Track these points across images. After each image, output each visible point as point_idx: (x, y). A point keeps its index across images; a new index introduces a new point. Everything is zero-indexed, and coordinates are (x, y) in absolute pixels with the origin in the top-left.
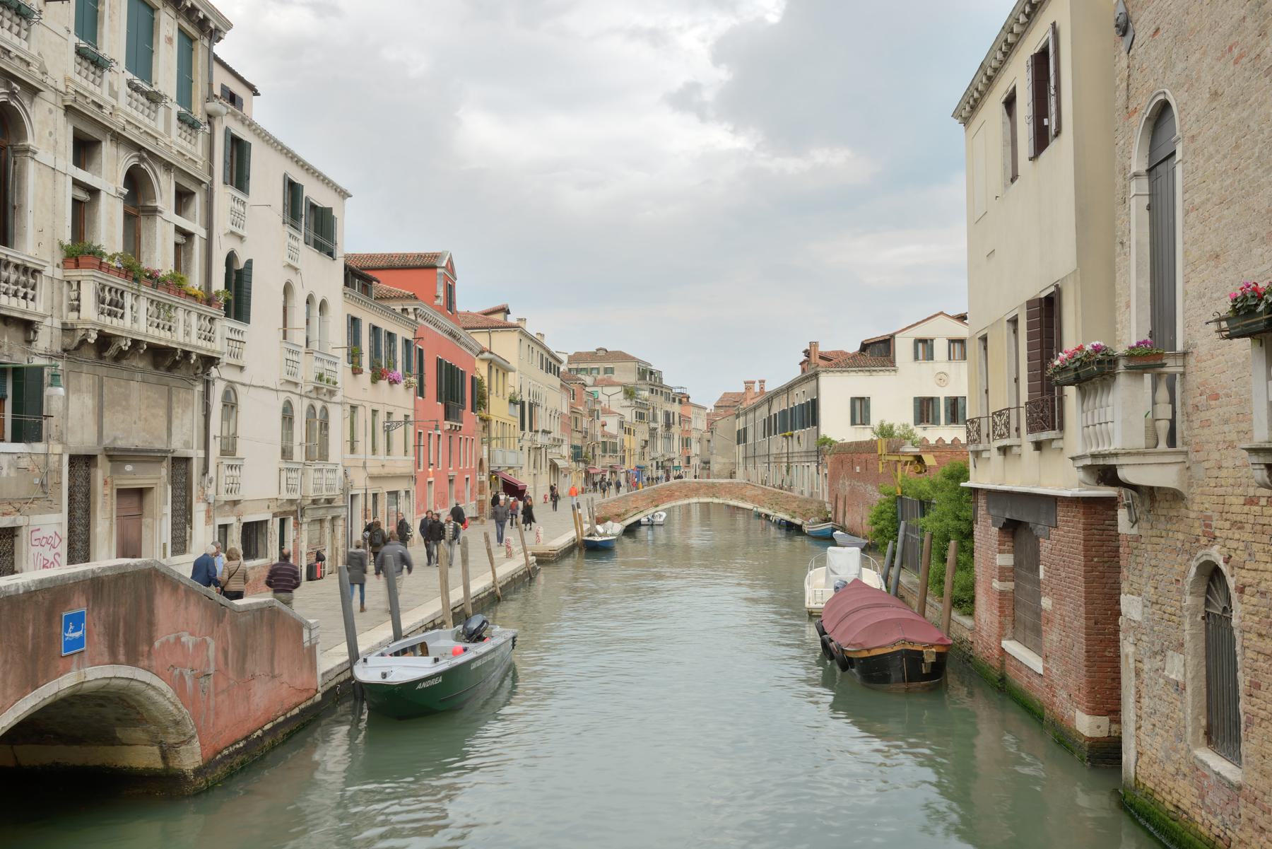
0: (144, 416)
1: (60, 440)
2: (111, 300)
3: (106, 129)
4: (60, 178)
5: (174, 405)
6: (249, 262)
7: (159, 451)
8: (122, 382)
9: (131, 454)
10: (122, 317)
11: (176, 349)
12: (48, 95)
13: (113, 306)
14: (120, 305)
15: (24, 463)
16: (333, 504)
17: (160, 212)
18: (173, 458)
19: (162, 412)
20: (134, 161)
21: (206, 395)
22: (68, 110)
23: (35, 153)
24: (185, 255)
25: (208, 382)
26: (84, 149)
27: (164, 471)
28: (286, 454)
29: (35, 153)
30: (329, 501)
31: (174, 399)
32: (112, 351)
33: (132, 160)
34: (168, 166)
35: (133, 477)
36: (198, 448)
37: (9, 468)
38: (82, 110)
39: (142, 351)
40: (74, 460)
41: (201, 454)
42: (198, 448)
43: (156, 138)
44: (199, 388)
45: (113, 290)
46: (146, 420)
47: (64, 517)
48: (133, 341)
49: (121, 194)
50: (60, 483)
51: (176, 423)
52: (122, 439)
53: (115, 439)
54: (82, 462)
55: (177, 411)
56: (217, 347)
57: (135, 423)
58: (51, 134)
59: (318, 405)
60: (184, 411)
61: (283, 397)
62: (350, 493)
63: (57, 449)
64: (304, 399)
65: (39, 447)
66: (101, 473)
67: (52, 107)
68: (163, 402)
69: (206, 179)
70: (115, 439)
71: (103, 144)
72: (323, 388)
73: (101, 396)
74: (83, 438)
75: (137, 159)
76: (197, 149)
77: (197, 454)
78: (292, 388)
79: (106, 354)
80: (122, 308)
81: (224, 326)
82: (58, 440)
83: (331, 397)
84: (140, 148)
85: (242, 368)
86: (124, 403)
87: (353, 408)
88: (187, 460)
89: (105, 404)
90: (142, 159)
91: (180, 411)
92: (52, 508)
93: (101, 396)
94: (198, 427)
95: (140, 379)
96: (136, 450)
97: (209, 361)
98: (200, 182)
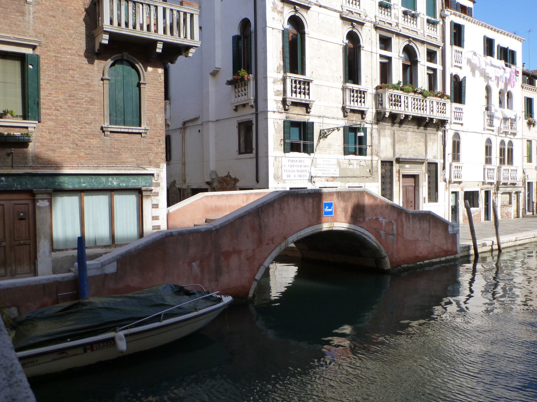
0: (413, 146)
1: (377, 155)
2: (395, 100)
3: (393, 32)
4: (374, 55)
5: (428, 141)
6: (465, 78)
7: (420, 159)
8: (404, 132)
9: (407, 160)
10: (400, 106)
11: (426, 117)
12: (367, 24)
13: (397, 101)
14: (399, 101)
15: (363, 163)
16: (516, 186)
17: (419, 62)
18: (429, 163)
19: (422, 144)
20: (407, 43)
21: (444, 137)
22: (376, 28)
23: (363, 47)
24: (433, 78)
25: (445, 131)
26: (385, 43)
27: (424, 167)
28: (488, 161)
29: (363, 47)
30: (514, 184)
31: (428, 138)
32: (398, 120)
33: (406, 43)
34: (423, 42)
35: (409, 169)
36: (441, 159)
37: (357, 165)
38: (382, 27)
39: (410, 119)
40: (383, 162)
41: (442, 161)
42: (441, 159)
43: (417, 32)
44: (440, 133)
45: (396, 96)
46: (415, 147)
47: (379, 184)
48: (405, 115)
49: (401, 57)
50: (378, 171)
51: (429, 149)
52: (404, 155)
53: (401, 155)
54: (387, 164)
55: (430, 144)
56: (447, 115)
57: (410, 148)
58: (370, 39)
59: (507, 141)
60: (433, 143)
61: (485, 137)
62: (527, 181)
63: (375, 158)
64: (498, 137)
65: (368, 158)
66: (396, 167)
67: (370, 28)
68: (423, 140)
69: (442, 45)
70: (401, 155)
71: (392, 39)
72: (508, 132)
73: (394, 138)
74: (388, 155)
75: (408, 42)
76: (438, 34)
77: (440, 162)
78: (491, 132)
79: (396, 121)
80: (400, 102)
81: (451, 107)
82: (376, 155)
83: (514, 137)
84: (408, 37)
85: (462, 124)
86: (405, 140)
87: (530, 141)
88: (436, 164)
89: (396, 141)
90: (410, 41)
91: (431, 143)
92: (374, 180)
93: (394, 138)
94: (440, 150)
95: (412, 131)
96: (409, 159)
97: (442, 123)
98: (438, 47)
